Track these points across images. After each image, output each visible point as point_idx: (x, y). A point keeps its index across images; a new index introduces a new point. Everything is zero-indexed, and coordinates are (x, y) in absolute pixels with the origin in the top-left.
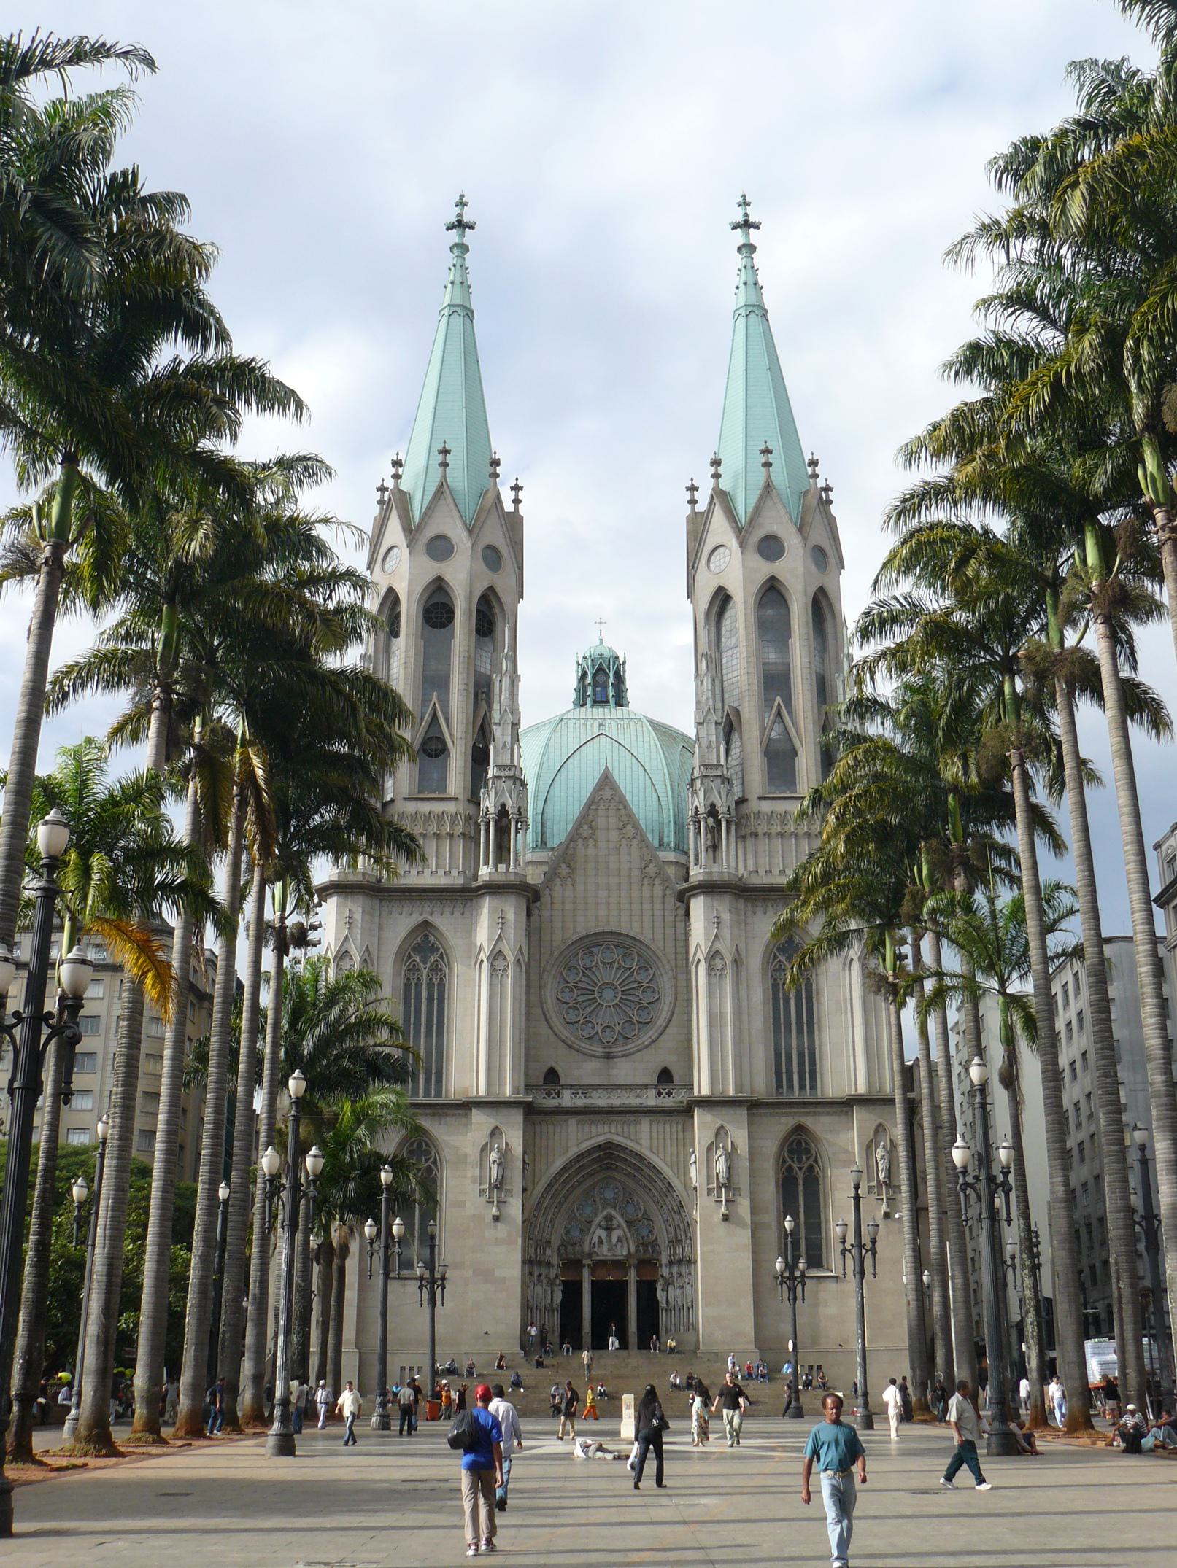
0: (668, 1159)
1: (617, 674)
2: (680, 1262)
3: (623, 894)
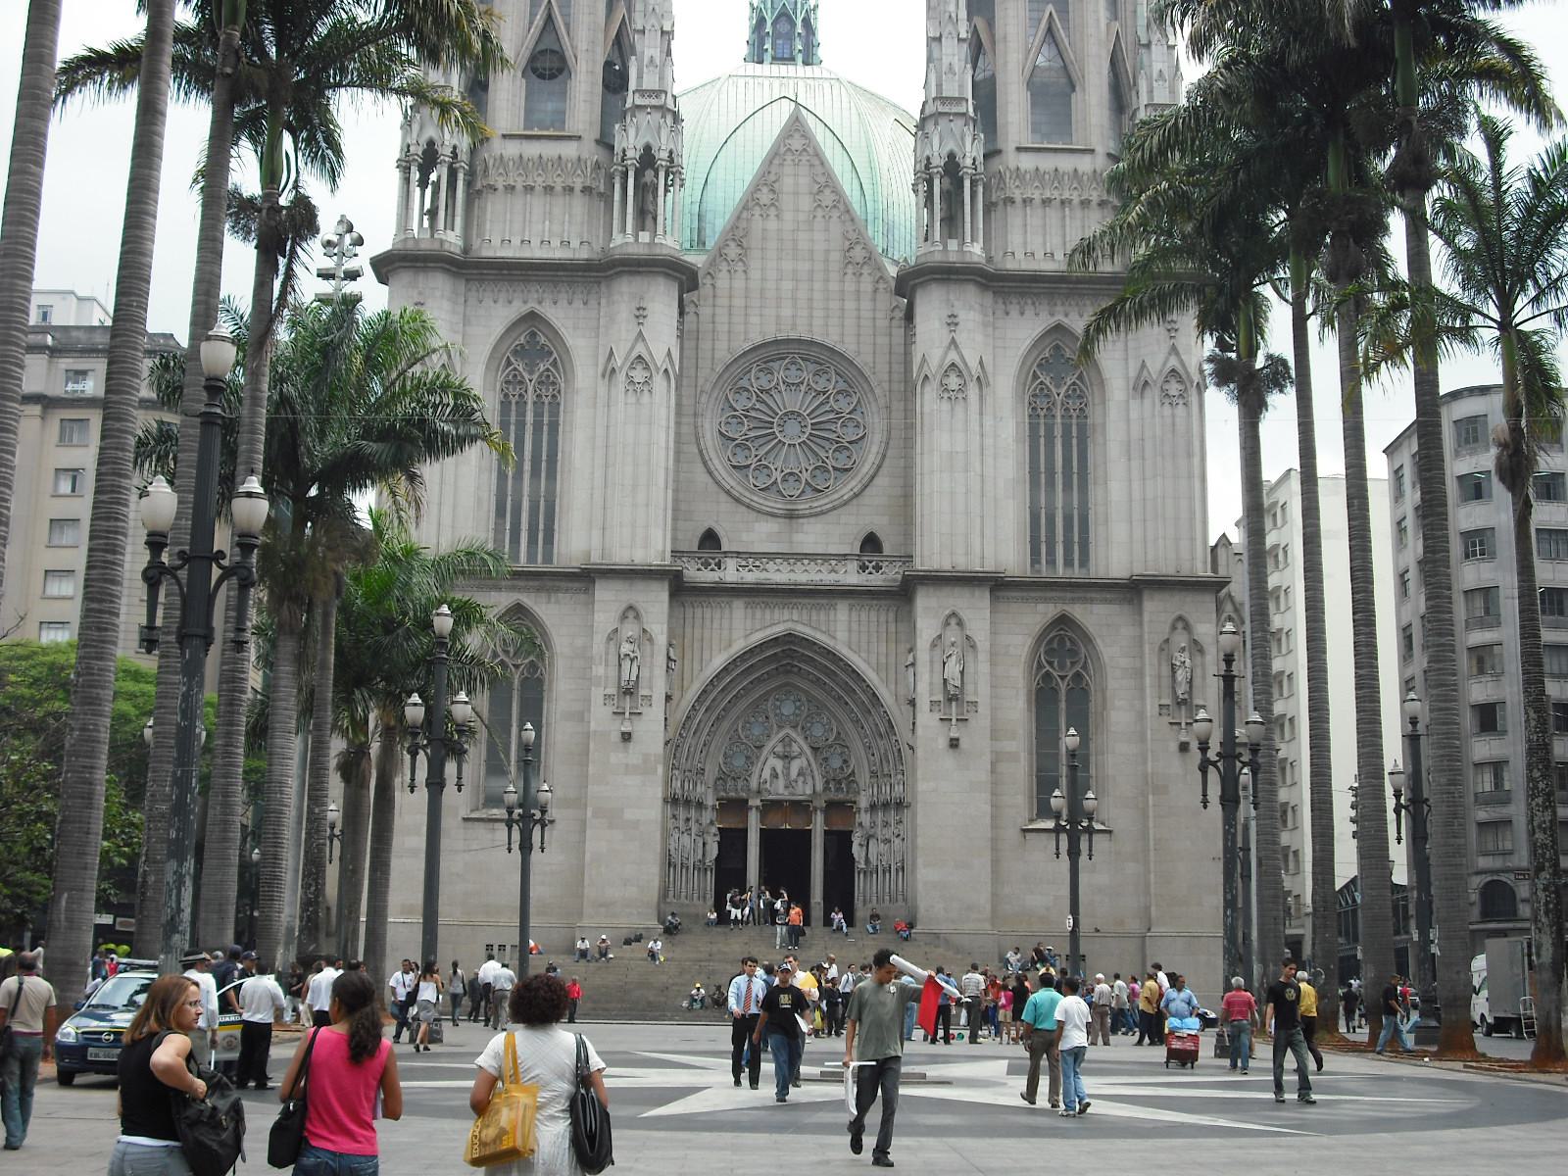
0: (874, 661)
1: (806, 22)
2: (886, 806)
3: (817, 286)
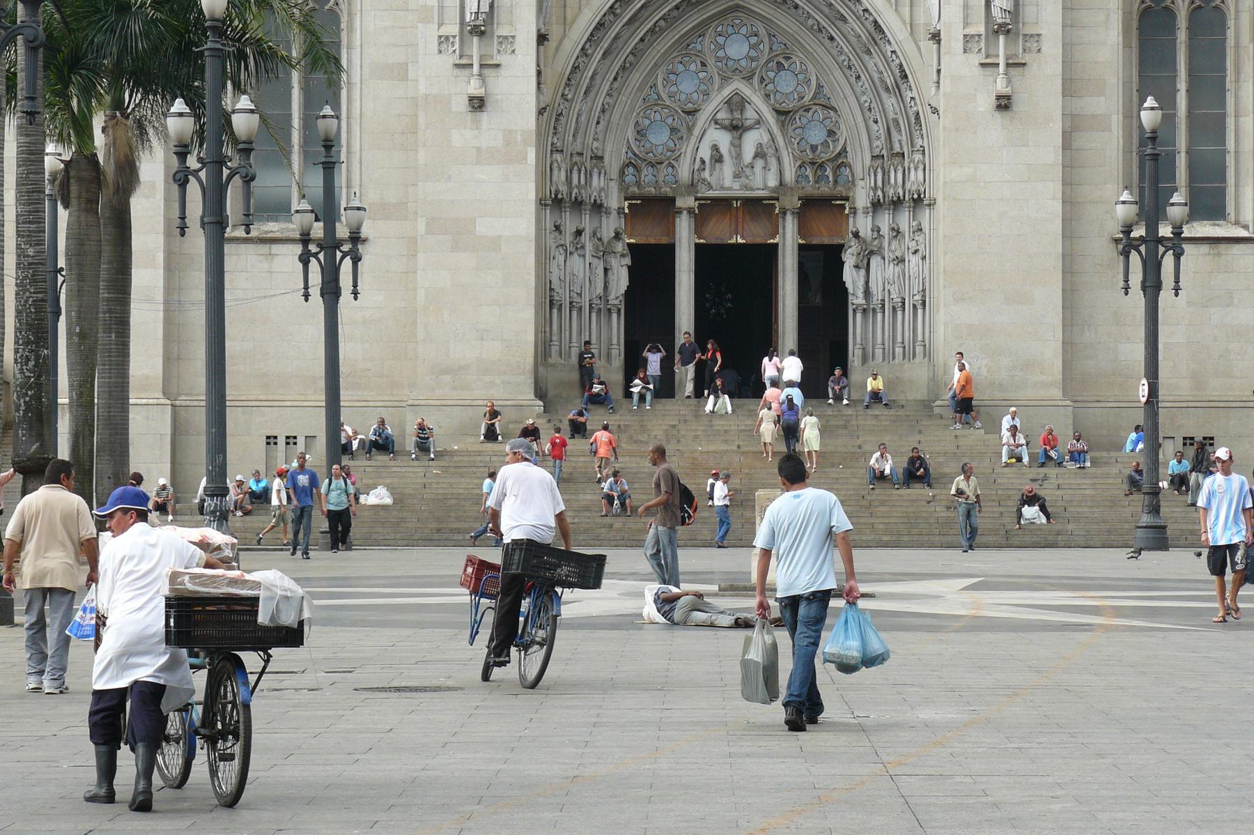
2: (897, 203)
